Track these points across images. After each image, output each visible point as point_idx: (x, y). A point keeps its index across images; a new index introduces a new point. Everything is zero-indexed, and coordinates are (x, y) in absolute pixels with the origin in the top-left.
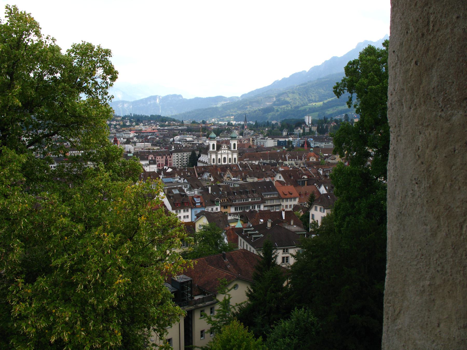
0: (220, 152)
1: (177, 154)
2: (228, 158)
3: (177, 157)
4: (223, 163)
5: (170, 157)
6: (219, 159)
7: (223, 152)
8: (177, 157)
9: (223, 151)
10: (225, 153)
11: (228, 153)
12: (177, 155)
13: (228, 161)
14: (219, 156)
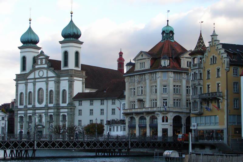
2: (47, 89)
4: (37, 105)
6: (30, 92)
7: (37, 76)
9: (37, 72)
10: (41, 78)
11: (47, 78)
13: (47, 99)
14: (30, 87)
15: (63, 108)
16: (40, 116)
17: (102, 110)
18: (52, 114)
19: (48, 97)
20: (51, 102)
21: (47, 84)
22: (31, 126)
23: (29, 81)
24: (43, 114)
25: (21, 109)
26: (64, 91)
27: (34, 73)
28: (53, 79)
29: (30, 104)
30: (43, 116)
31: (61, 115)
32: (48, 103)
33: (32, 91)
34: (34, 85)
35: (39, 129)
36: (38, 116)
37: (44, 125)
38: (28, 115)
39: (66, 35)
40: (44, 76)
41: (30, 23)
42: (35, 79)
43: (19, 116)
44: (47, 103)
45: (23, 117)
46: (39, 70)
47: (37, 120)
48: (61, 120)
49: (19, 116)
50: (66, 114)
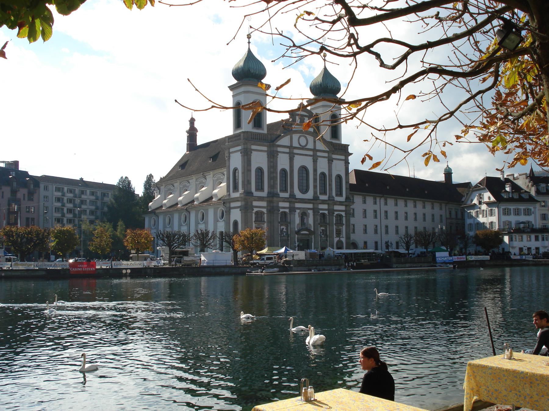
0: (285, 141)
1: (58, 189)
2: (315, 170)
3: (58, 200)
5: (31, 199)
7: (295, 144)
8: (58, 200)
10: (303, 148)
12: (59, 194)
13: (315, 187)
14: (283, 162)
15: (341, 203)
16: (304, 215)
17: (375, 211)
18: (326, 212)
19: (316, 182)
20: (324, 192)
21: (315, 162)
22: (284, 230)
23: (279, 149)
24: (311, 212)
25: (260, 199)
26: (339, 177)
27: (289, 136)
28: (326, 155)
29: (285, 190)
30: (309, 213)
31: (335, 215)
32: (317, 193)
33: (288, 169)
34: (291, 160)
35: (303, 236)
36: (300, 214)
37: (312, 230)
38: (281, 210)
39: (334, 88)
40: (307, 147)
41: (249, 43)
42: (291, 147)
43: (254, 211)
44: (315, 193)
45: (264, 213)
46: (300, 135)
47: (297, 220)
48: (334, 222)
49: (254, 211)
50: (343, 214)
